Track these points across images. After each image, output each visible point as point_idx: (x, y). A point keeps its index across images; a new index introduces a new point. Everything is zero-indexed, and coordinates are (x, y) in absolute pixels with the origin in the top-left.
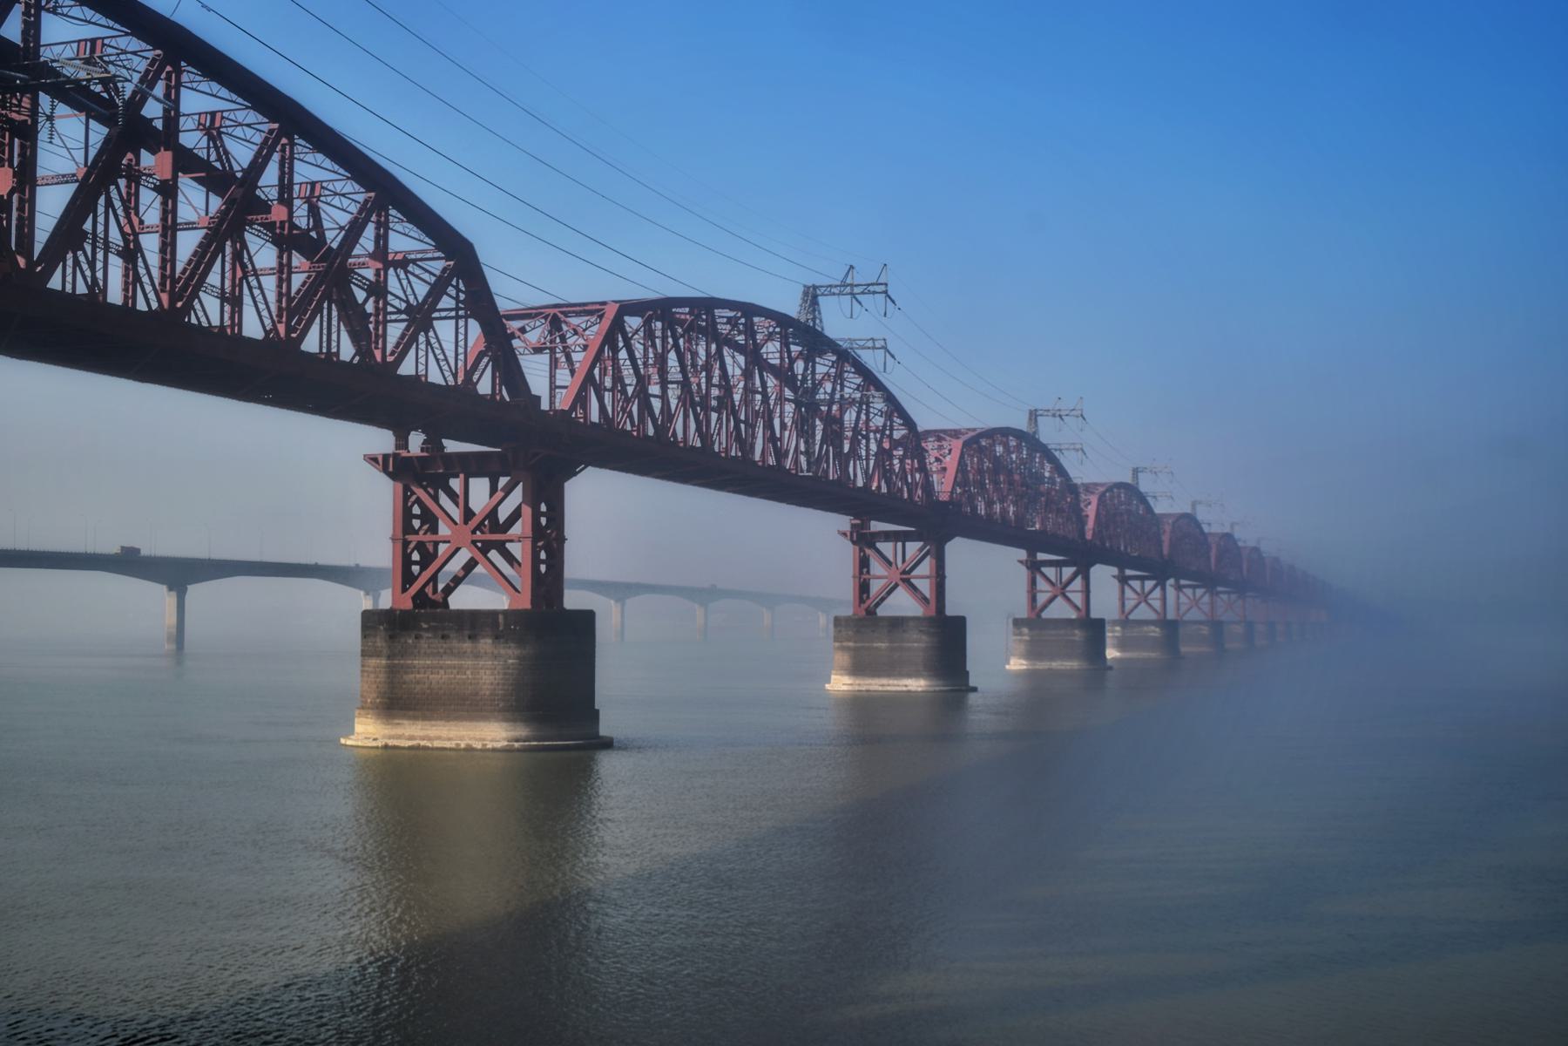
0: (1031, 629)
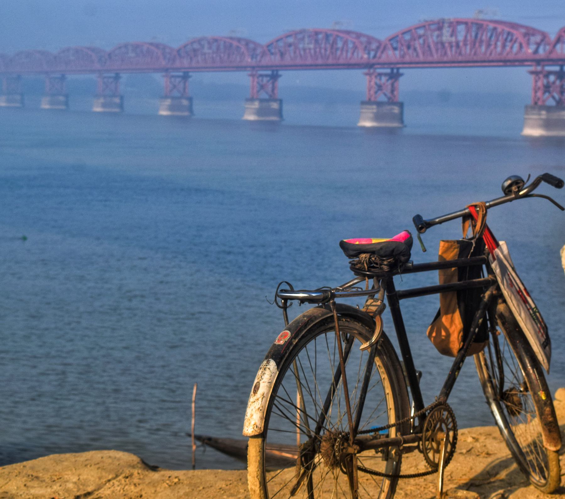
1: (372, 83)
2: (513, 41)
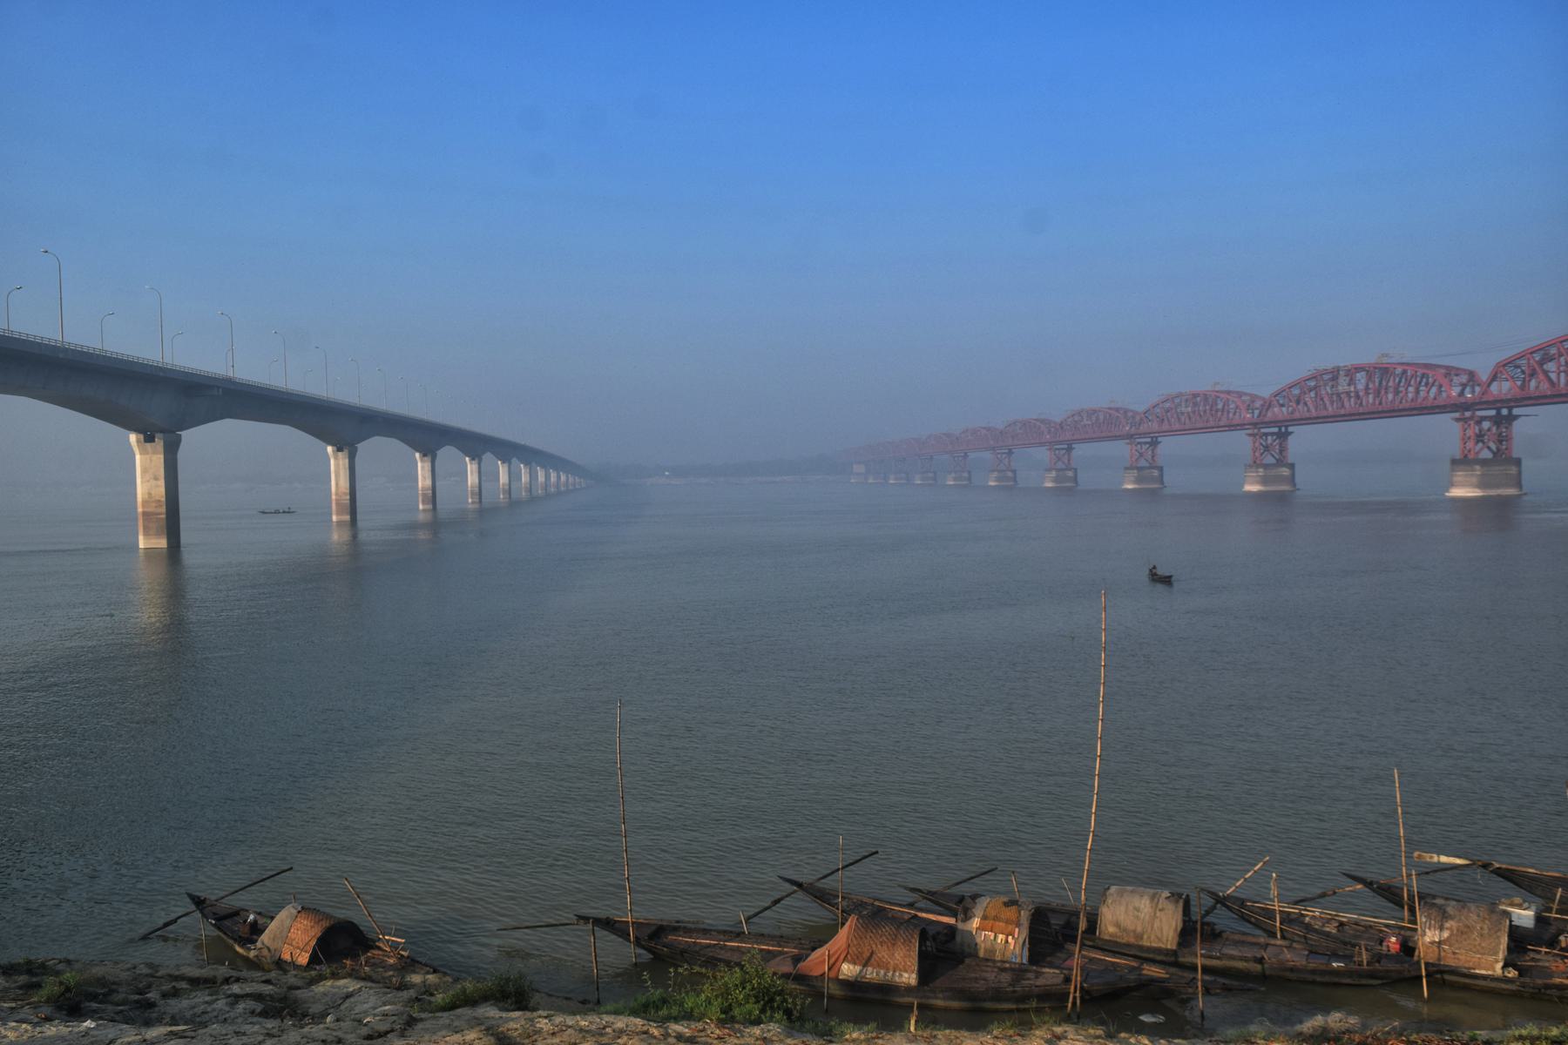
1: (1257, 444)
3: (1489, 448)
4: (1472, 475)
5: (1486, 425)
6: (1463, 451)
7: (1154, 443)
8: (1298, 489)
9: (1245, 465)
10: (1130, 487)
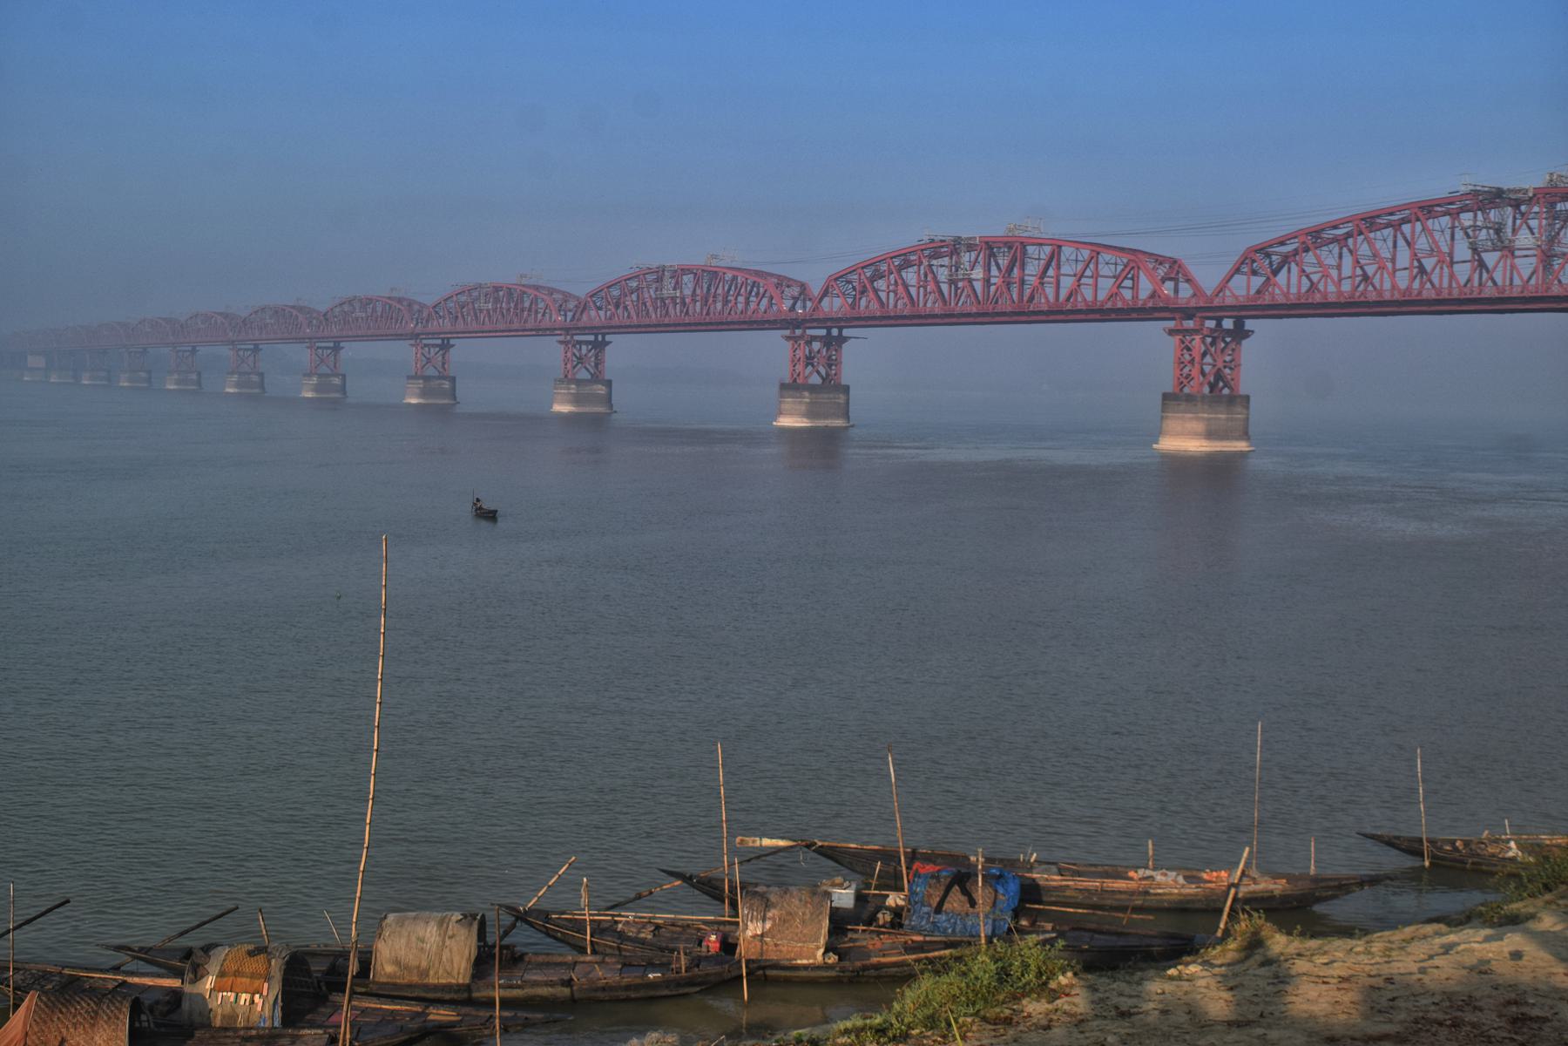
0: (811, 393)
1: (569, 354)
2: (760, 297)
3: (818, 372)
4: (800, 402)
5: (816, 346)
6: (792, 375)
7: (445, 346)
8: (615, 412)
9: (555, 380)
10: (414, 401)
